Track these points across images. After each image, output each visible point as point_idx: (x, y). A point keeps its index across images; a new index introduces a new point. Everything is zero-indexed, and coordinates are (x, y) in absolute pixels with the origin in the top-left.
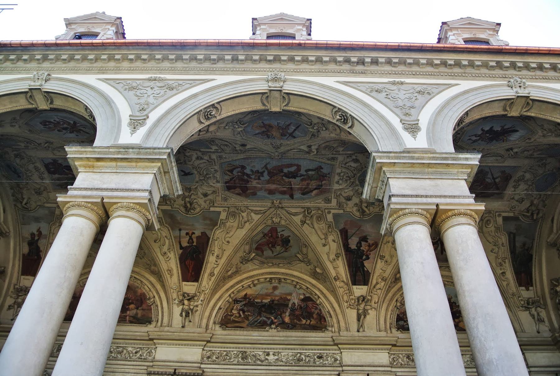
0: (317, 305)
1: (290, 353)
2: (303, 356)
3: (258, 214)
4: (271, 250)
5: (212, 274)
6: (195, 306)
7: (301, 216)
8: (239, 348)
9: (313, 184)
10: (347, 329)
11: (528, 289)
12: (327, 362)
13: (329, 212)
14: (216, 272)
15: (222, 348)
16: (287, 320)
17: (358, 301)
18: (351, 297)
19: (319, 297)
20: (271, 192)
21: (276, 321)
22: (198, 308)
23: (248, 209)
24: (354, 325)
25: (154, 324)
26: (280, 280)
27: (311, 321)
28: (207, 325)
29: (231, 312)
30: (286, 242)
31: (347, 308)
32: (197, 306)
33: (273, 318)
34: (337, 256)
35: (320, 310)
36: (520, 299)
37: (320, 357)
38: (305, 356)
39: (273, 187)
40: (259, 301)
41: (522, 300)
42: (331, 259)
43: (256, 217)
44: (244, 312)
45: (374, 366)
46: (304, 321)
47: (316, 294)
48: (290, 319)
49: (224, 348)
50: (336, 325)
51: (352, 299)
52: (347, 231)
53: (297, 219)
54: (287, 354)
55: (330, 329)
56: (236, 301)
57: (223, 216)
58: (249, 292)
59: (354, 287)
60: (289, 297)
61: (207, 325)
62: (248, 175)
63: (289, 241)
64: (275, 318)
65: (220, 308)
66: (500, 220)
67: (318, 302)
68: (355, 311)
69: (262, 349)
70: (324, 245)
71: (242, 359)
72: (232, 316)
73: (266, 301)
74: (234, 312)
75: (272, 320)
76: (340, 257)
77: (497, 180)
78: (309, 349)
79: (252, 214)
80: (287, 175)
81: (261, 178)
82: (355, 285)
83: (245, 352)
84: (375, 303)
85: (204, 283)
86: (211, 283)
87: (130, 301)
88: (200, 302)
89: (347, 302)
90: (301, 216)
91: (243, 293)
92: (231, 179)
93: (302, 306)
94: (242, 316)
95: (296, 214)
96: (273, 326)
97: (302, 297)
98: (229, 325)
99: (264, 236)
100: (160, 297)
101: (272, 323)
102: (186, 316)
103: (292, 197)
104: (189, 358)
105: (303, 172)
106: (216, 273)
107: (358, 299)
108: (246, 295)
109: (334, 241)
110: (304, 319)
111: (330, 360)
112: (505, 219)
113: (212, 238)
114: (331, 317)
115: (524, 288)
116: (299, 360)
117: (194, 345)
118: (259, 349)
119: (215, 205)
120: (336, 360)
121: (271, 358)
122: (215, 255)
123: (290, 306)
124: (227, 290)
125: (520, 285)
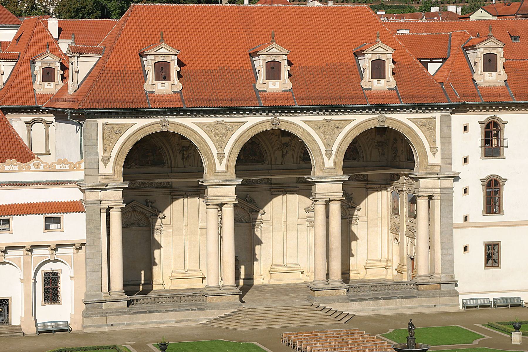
6: (189, 154)
12: (264, 182)
17: (283, 147)
22: (192, 155)
25: (166, 166)
35: (261, 150)
48: (244, 156)
55: (266, 162)
59: (282, 138)
67: (260, 145)
68: (281, 152)
84: (293, 146)
87: (148, 151)
100: (166, 147)
110: (251, 156)
114: (267, 154)
115: (379, 136)
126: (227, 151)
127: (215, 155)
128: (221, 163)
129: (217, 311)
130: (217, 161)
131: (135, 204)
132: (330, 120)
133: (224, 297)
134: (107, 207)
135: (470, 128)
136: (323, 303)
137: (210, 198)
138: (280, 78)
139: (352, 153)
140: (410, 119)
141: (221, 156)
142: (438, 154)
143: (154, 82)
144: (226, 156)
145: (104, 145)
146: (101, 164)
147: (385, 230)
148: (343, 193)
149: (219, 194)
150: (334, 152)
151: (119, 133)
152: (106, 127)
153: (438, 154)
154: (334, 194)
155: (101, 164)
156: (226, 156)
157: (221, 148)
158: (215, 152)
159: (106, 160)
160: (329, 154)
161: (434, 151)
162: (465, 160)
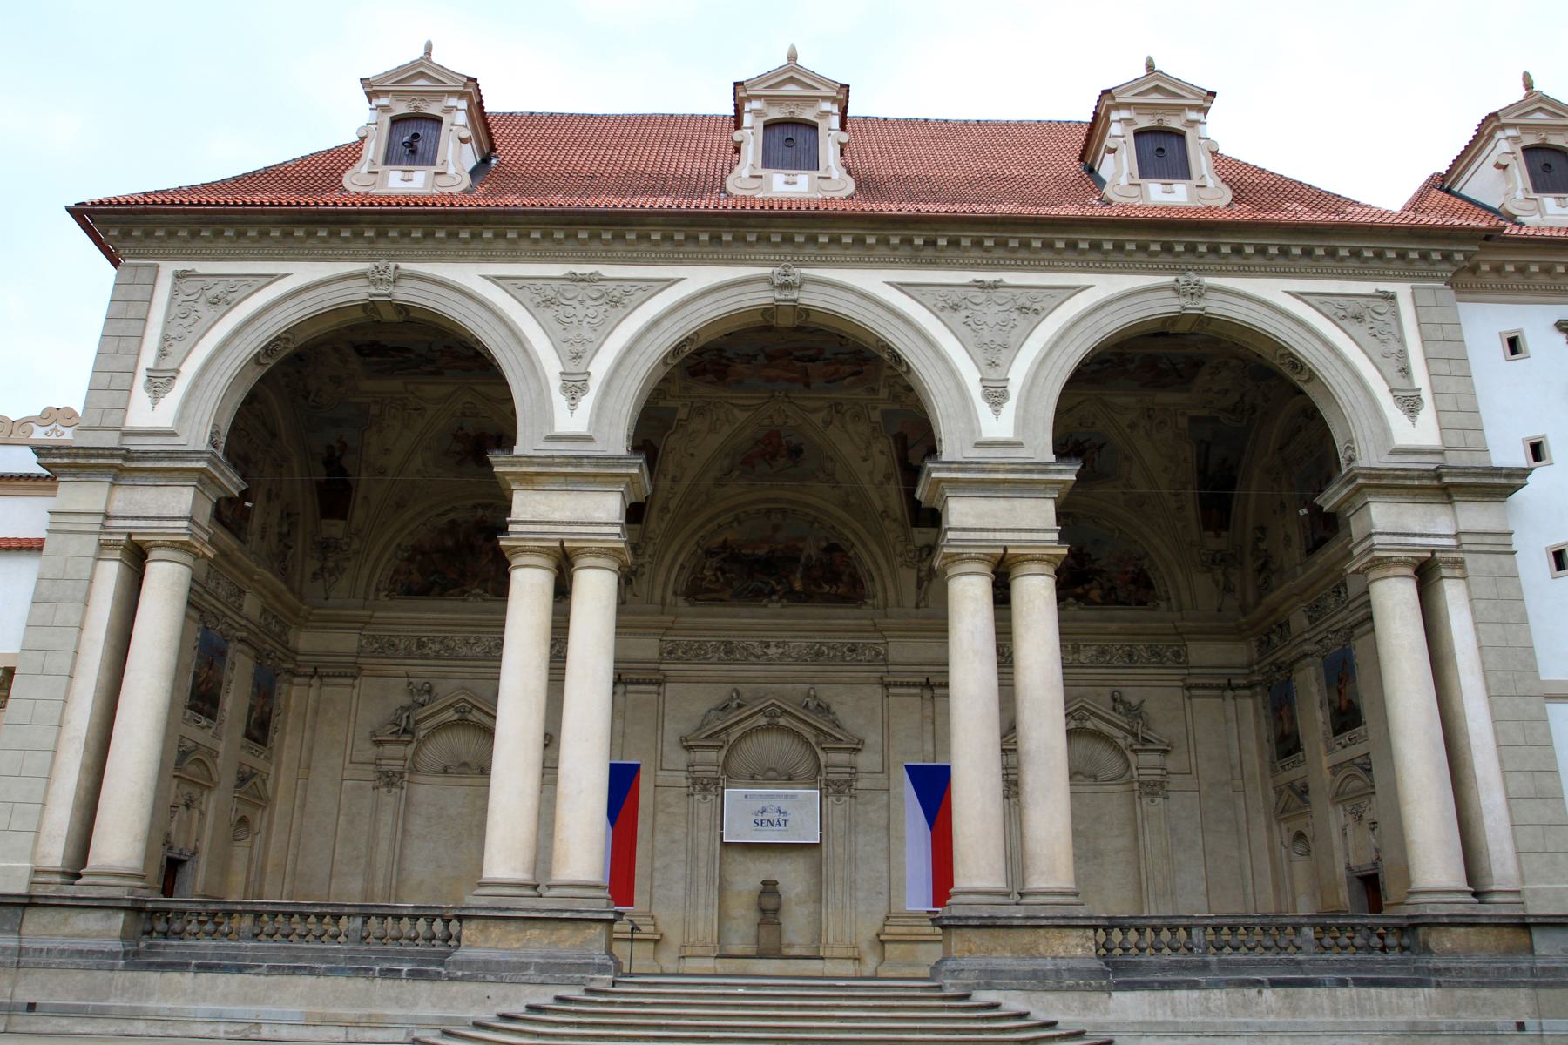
0: (850, 558)
1: (804, 642)
2: (824, 648)
3: (746, 410)
4: (769, 464)
5: (665, 509)
6: (638, 566)
7: (823, 414)
8: (719, 637)
9: (848, 369)
10: (899, 604)
11: (1218, 536)
12: (863, 657)
13: (875, 408)
14: (672, 505)
15: (691, 636)
16: (798, 586)
17: (920, 555)
18: (909, 547)
19: (853, 545)
20: (769, 380)
21: (778, 588)
22: (646, 570)
23: (726, 402)
24: (910, 594)
26: (784, 511)
27: (838, 587)
28: (663, 598)
29: (702, 573)
30: (796, 452)
31: (901, 566)
32: (642, 565)
33: (773, 583)
34: (888, 477)
35: (855, 568)
36: (1201, 551)
37: (852, 650)
38: (828, 648)
39: (773, 373)
40: (748, 551)
41: (1204, 554)
42: (876, 482)
43: (742, 416)
44: (724, 573)
45: (939, 665)
46: (827, 588)
47: (847, 539)
49: (695, 636)
50: (880, 595)
51: (911, 551)
52: (905, 438)
53: (817, 418)
54: (798, 645)
55: (870, 602)
56: (709, 553)
57: (682, 414)
58: (730, 535)
59: (915, 530)
60: (801, 545)
61: (663, 598)
62: (729, 359)
63: (801, 451)
64: (778, 584)
65: (682, 567)
66: (1183, 422)
67: (851, 553)
68: (915, 571)
69: (758, 637)
70: (865, 460)
71: (726, 653)
72: (703, 579)
73: (762, 552)
74: (708, 573)
75: (773, 588)
76: (892, 482)
77: (1179, 367)
78: (835, 638)
79: (736, 411)
80: (798, 359)
81: (754, 362)
82: (916, 526)
83: (731, 643)
85: (652, 525)
86: (663, 526)
88: (647, 559)
89: (901, 556)
90: (823, 414)
91: (720, 539)
92: (698, 364)
93: (824, 561)
94: (721, 580)
95: (815, 410)
96: (775, 597)
97: (824, 544)
98: (699, 597)
99: (756, 444)
101: (773, 592)
102: (626, 583)
103: (808, 385)
104: (640, 655)
105: (827, 355)
106: (672, 505)
107: (921, 549)
108: (725, 541)
109: (882, 453)
111: (868, 654)
112: (1194, 420)
113: (664, 450)
114: (872, 580)
115: (1211, 533)
116: (819, 654)
117: (645, 634)
118: (753, 637)
119: (668, 398)
120: (878, 654)
121: (773, 651)
122: (669, 477)
123: (803, 560)
124: (694, 533)
125: (1206, 528)
126: (600, 367)
127: (555, 384)
128: (573, 400)
129: (492, 990)
130: (559, 401)
131: (465, 701)
132: (995, 286)
133: (534, 932)
134: (124, 537)
135: (1529, 342)
136: (989, 987)
137: (519, 528)
138: (815, 165)
139: (1132, 587)
140: (1299, 296)
141: (574, 386)
142: (1427, 414)
143: (380, 168)
144: (595, 385)
145: (165, 337)
146: (140, 396)
147: (1260, 821)
148: (1061, 534)
149: (556, 517)
150: (1015, 386)
151: (221, 303)
152: (189, 286)
153: (1427, 414)
154: (1024, 536)
155: (140, 396)
156: (595, 385)
157: (576, 353)
158: (552, 366)
159: (159, 383)
160: (996, 395)
161: (1411, 404)
162: (1537, 451)
